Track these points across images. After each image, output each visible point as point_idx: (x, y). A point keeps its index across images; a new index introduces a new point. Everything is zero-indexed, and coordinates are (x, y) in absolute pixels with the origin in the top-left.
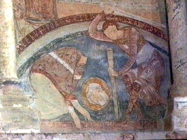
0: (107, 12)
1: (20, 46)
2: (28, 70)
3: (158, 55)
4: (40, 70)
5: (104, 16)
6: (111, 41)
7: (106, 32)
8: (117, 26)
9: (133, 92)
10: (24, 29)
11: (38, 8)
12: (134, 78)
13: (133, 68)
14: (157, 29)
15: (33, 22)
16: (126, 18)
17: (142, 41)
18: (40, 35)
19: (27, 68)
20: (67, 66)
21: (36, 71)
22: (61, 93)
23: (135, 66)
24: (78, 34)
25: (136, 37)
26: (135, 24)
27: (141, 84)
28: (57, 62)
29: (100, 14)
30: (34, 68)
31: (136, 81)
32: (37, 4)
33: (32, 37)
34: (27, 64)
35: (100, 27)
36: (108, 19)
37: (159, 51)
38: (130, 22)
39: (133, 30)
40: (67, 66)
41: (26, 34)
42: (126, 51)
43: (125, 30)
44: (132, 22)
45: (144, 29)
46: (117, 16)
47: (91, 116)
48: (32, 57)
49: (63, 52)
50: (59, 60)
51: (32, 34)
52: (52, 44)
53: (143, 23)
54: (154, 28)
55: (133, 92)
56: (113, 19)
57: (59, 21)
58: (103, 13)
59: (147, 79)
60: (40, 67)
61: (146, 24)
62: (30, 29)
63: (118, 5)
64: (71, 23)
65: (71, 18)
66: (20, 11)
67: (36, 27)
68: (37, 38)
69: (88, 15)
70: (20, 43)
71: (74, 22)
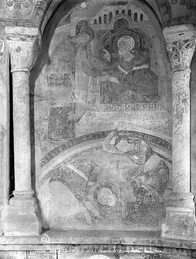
0: (120, 129)
1: (42, 162)
2: (49, 180)
3: (164, 164)
4: (58, 179)
5: (117, 132)
6: (122, 153)
7: (118, 146)
8: (128, 140)
9: (139, 195)
10: (45, 149)
11: (59, 131)
12: (141, 183)
13: (141, 175)
14: (165, 141)
15: (54, 142)
16: (137, 132)
17: (150, 152)
18: (59, 152)
19: (48, 178)
20: (82, 174)
21: (55, 180)
22: (76, 196)
23: (142, 174)
24: (93, 149)
25: (145, 149)
26: (145, 137)
27: (147, 189)
28: (73, 172)
29: (114, 131)
30: (54, 177)
31: (142, 186)
32: (59, 127)
33: (53, 154)
34: (48, 175)
35: (113, 142)
36: (120, 134)
37: (165, 161)
38: (140, 136)
39: (143, 142)
40: (82, 174)
41: (48, 152)
42: (136, 161)
43: (135, 143)
44: (143, 136)
45: (152, 141)
46: (129, 132)
47: (101, 214)
48: (52, 170)
49: (79, 164)
50: (75, 170)
51: (53, 151)
52: (69, 159)
53: (153, 136)
54: (162, 140)
55: (139, 195)
56: (125, 134)
57: (76, 140)
58: (116, 130)
59: (152, 185)
60: (59, 177)
61: (155, 137)
62: (52, 148)
63: (131, 122)
64: (87, 140)
65: (87, 136)
66: (43, 134)
67: (56, 146)
68: (57, 155)
69: (103, 132)
70: (42, 159)
71: (90, 139)
